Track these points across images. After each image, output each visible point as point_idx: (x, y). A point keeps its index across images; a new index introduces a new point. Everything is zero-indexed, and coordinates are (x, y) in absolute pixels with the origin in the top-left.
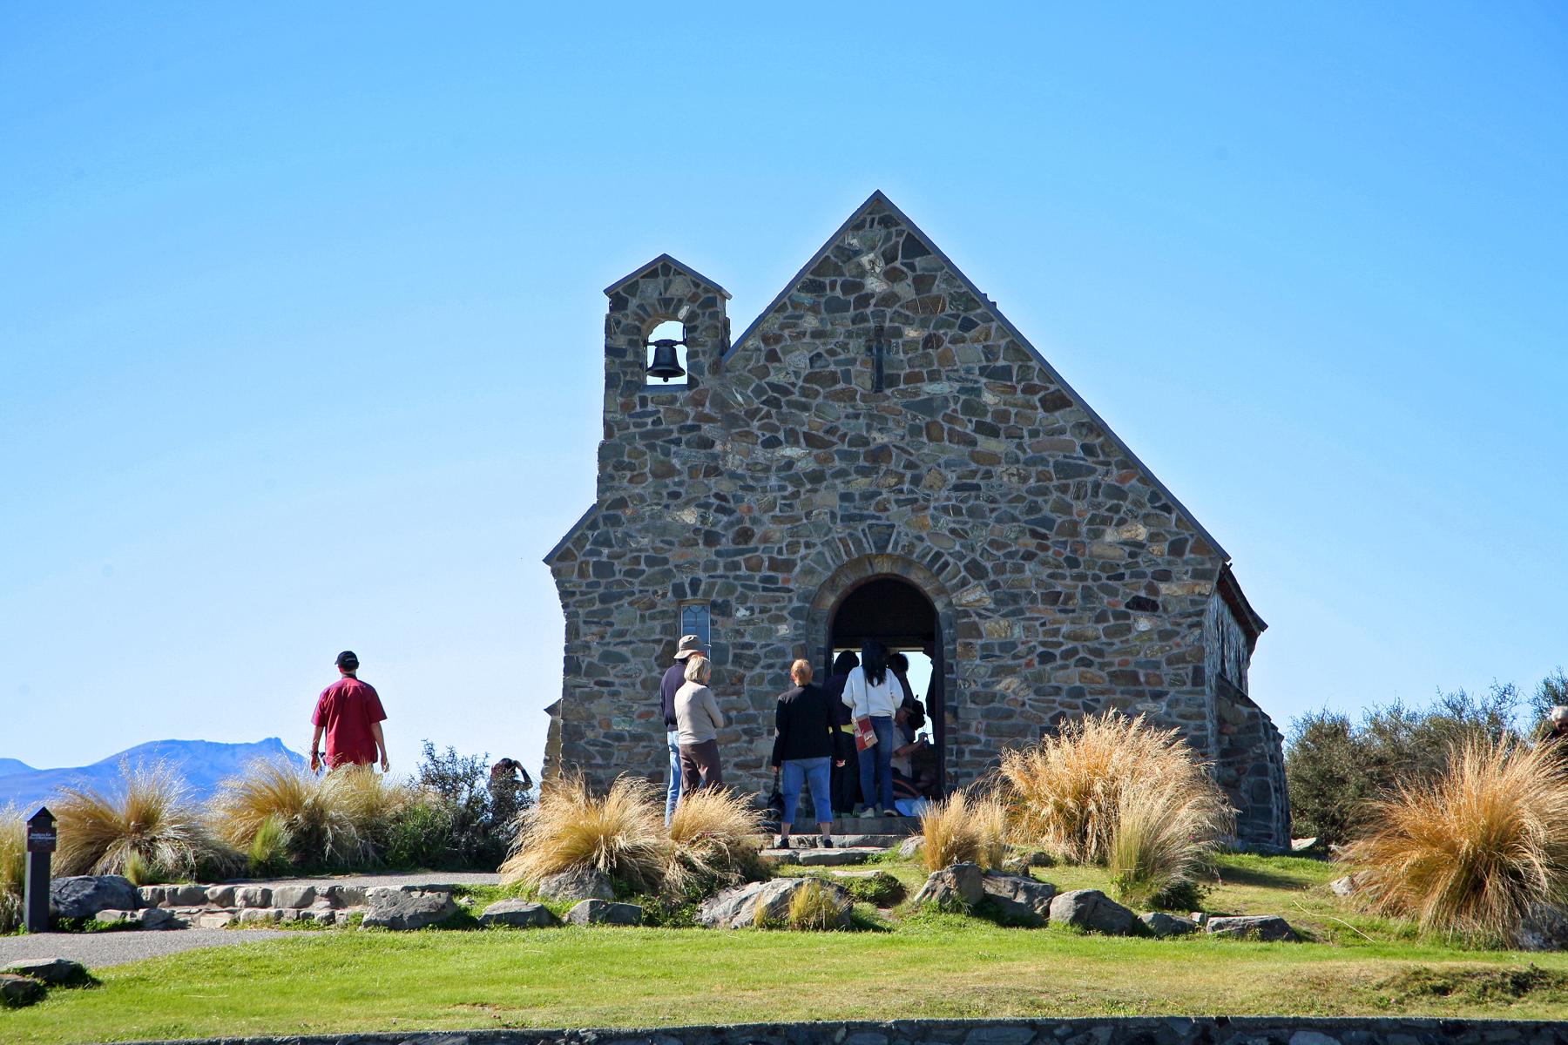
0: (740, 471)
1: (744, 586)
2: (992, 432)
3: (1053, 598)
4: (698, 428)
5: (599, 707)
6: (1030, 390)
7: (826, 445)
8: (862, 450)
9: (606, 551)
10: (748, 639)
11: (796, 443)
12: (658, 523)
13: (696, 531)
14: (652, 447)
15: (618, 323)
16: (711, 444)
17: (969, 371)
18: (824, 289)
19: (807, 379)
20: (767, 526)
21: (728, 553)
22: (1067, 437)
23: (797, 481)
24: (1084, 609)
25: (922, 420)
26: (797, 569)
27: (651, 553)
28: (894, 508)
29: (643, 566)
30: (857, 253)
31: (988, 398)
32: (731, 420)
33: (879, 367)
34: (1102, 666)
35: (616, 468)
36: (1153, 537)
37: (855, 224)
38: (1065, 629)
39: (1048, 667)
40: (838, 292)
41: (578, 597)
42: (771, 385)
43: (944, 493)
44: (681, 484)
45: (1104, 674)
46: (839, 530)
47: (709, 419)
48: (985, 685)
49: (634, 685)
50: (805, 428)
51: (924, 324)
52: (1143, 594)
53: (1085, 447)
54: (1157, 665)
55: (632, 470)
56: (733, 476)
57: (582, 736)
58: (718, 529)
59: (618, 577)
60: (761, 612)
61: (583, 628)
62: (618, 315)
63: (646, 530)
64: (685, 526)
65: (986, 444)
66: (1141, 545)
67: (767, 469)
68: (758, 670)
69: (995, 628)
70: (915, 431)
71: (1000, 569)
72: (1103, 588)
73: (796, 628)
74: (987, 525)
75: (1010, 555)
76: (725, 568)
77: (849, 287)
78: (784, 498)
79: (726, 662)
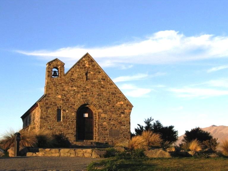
0: (67, 90)
2: (103, 87)
3: (111, 111)
6: (108, 82)
7: (80, 87)
8: (85, 89)
9: (47, 101)
10: (68, 115)
11: (76, 87)
12: (55, 97)
13: (61, 99)
14: (54, 86)
15: (50, 67)
16: (63, 86)
17: (100, 79)
18: (80, 65)
19: (78, 78)
21: (65, 102)
22: (113, 89)
25: (93, 85)
26: (75, 105)
29: (53, 103)
30: (85, 61)
31: (102, 83)
32: (66, 83)
33: (87, 77)
34: (117, 121)
35: (49, 89)
36: (124, 103)
37: (85, 56)
39: (110, 121)
40: (82, 66)
42: (72, 78)
43: (96, 96)
44: (58, 92)
45: (117, 122)
46: (82, 100)
47: (63, 83)
49: (51, 121)
50: (77, 85)
52: (123, 111)
53: (115, 91)
54: (124, 121)
56: (66, 91)
59: (49, 105)
61: (43, 112)
62: (49, 66)
63: (54, 98)
64: (59, 98)
65: (102, 89)
66: (122, 105)
67: (71, 90)
69: (103, 115)
71: (104, 107)
73: (75, 114)
74: (102, 101)
77: (83, 66)
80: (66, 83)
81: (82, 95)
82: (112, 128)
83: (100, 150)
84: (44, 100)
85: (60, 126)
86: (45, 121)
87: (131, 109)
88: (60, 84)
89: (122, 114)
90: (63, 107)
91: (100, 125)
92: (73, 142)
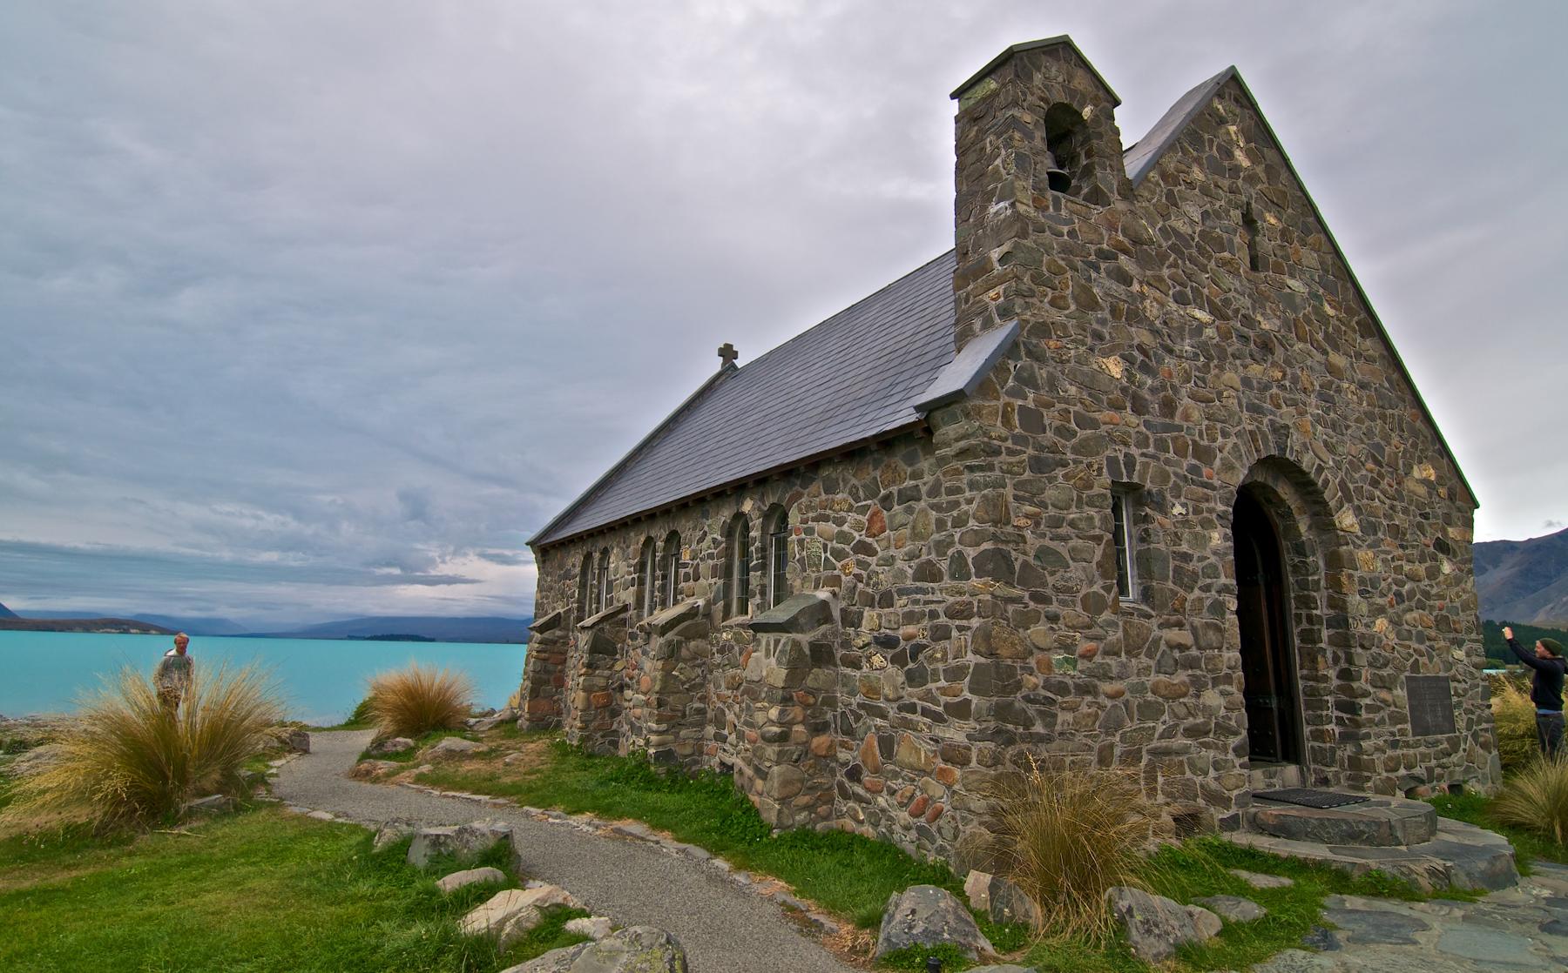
1: (1176, 474)
2: (1336, 348)
3: (1396, 531)
5: (1038, 632)
7: (1225, 318)
10: (1184, 548)
13: (1124, 390)
19: (1202, 234)
24: (1413, 547)
25: (1291, 315)
26: (1217, 462)
27: (1079, 407)
28: (1285, 409)
31: (1330, 311)
38: (1407, 568)
41: (1004, 457)
42: (1174, 230)
43: (1313, 400)
44: (1103, 322)
47: (1126, 252)
48: (1367, 626)
54: (1455, 611)
55: (1054, 289)
57: (1019, 686)
60: (1197, 511)
65: (1338, 360)
67: (1181, 329)
68: (1197, 592)
70: (1286, 324)
73: (1226, 538)
76: (1156, 447)
78: (1198, 369)
79: (1166, 578)
81: (1246, 382)
82: (1415, 667)
84: (1011, 383)
85: (1143, 658)
86: (1032, 604)
89: (1440, 555)
90: (1145, 466)
92: (1233, 811)
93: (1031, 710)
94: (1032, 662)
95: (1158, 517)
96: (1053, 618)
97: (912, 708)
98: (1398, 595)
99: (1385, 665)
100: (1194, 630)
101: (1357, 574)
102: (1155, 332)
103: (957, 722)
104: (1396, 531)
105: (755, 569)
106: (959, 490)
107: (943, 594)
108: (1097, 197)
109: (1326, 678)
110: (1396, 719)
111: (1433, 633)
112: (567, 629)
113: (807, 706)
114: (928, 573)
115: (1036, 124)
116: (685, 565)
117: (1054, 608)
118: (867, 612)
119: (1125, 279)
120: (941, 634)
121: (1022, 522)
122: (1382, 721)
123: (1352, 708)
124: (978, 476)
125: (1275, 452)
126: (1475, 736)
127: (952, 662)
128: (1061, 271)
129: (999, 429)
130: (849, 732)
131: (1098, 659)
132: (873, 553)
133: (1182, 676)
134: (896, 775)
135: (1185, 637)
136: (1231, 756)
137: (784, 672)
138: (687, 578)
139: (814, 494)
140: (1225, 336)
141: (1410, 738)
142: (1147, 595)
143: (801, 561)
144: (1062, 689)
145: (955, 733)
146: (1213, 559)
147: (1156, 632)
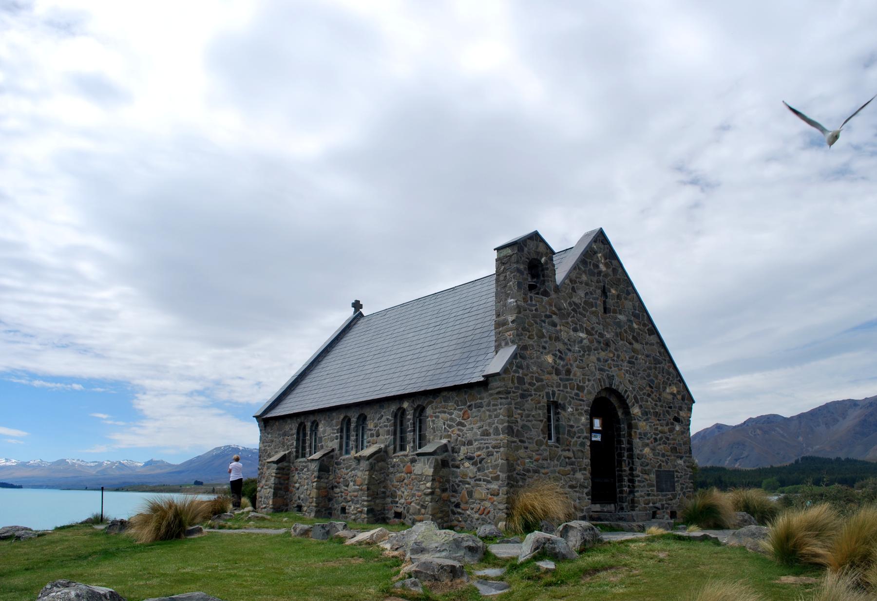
2: (637, 341)
3: (656, 414)
4: (551, 317)
5: (521, 453)
6: (645, 325)
7: (592, 335)
10: (572, 423)
11: (583, 332)
13: (553, 367)
19: (585, 303)
20: (575, 369)
23: (583, 348)
26: (586, 391)
27: (537, 375)
31: (635, 326)
36: (678, 392)
38: (660, 428)
41: (512, 394)
43: (626, 364)
44: (546, 342)
47: (555, 314)
51: (616, 290)
56: (565, 344)
57: (515, 470)
58: (560, 368)
61: (514, 410)
65: (637, 346)
67: (575, 341)
70: (617, 335)
72: (668, 412)
73: (587, 419)
75: (644, 394)
79: (564, 434)
80: (563, 316)
82: (660, 466)
83: (680, 538)
85: (556, 462)
87: (690, 410)
88: (550, 317)
91: (638, 454)
93: (518, 477)
94: (519, 462)
95: (563, 412)
96: (526, 448)
97: (480, 480)
98: (655, 440)
99: (647, 465)
100: (574, 452)
101: (638, 431)
102: (565, 344)
103: (495, 482)
104: (656, 414)
105: (410, 431)
106: (496, 405)
107: (492, 440)
108: (546, 294)
109: (625, 471)
110: (651, 485)
111: (669, 453)
112: (289, 462)
113: (440, 482)
114: (486, 434)
115: (525, 269)
116: (370, 430)
117: (526, 444)
118: (462, 448)
119: (554, 325)
120: (490, 454)
121: (517, 416)
122: (644, 486)
123: (632, 481)
124: (503, 401)
125: (608, 386)
126: (684, 493)
127: (494, 463)
128: (532, 325)
129: (511, 385)
130: (455, 491)
131: (540, 461)
132: (464, 426)
133: (569, 468)
134: (474, 503)
135: (570, 454)
136: (585, 495)
137: (432, 470)
138: (372, 435)
139: (438, 402)
140: (591, 342)
141: (655, 493)
142: (558, 440)
143: (433, 428)
144: (528, 471)
145: (494, 486)
146: (582, 427)
147: (560, 453)
